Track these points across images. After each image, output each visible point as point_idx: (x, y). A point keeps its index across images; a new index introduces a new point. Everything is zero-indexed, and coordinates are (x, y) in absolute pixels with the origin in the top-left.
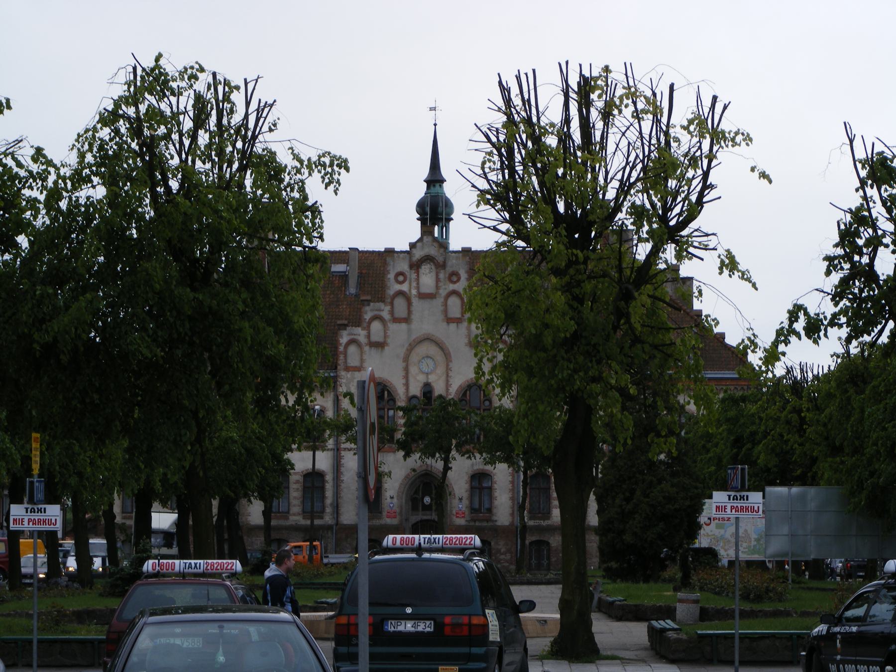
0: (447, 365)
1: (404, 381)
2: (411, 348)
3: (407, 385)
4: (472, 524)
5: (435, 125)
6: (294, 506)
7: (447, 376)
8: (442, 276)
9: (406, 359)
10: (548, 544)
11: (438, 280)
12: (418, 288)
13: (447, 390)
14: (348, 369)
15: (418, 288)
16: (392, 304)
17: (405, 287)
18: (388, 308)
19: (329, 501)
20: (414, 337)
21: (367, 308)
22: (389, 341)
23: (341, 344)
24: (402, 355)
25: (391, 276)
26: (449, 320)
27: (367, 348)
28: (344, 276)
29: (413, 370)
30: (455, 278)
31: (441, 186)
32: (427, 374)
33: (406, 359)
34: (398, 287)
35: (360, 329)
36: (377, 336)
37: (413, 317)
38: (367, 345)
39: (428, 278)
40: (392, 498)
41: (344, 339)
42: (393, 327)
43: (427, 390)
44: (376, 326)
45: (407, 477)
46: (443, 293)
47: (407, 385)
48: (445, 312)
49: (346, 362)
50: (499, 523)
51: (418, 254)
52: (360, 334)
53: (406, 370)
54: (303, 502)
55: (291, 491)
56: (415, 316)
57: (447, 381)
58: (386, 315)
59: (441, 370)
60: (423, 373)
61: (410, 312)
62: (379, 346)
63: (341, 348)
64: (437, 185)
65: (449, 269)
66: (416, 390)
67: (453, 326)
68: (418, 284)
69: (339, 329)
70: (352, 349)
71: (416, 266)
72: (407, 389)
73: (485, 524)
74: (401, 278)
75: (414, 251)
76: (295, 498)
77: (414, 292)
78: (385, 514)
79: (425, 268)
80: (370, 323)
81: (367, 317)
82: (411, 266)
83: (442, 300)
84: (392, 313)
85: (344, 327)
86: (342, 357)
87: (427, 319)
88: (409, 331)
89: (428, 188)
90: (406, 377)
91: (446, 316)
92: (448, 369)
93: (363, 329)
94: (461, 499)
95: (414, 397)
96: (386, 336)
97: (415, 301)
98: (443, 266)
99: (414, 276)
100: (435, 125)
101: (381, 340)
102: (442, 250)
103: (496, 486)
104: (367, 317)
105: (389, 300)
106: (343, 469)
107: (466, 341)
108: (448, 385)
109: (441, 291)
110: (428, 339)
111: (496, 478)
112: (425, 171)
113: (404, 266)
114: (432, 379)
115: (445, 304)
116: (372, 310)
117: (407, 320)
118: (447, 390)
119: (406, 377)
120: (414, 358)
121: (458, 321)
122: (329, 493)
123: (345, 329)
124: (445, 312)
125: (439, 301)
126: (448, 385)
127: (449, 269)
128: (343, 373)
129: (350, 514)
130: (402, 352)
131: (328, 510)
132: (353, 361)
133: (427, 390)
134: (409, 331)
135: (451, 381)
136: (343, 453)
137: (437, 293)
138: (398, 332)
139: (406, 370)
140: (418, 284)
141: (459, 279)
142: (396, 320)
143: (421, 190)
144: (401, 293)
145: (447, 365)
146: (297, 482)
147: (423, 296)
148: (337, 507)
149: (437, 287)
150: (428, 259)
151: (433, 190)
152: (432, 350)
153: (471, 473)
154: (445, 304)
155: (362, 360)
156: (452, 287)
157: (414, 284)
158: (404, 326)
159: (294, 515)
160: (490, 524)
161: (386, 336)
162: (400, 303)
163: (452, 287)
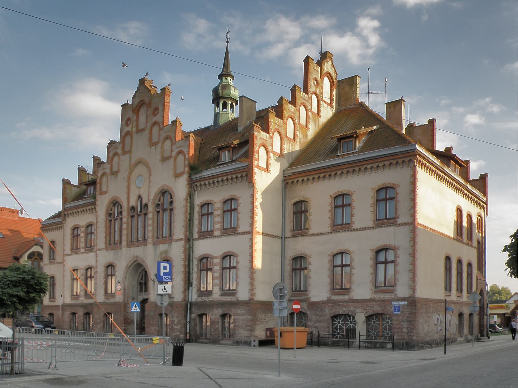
0: (149, 179)
1: (126, 196)
9: (129, 180)
29: (133, 187)
33: (129, 180)
48: (150, 139)
53: (129, 187)
77: (134, 130)
88: (130, 158)
92: (150, 182)
117: (130, 152)
124: (150, 139)
125: (147, 131)
134: (130, 158)
139: (129, 187)
156: (154, 119)
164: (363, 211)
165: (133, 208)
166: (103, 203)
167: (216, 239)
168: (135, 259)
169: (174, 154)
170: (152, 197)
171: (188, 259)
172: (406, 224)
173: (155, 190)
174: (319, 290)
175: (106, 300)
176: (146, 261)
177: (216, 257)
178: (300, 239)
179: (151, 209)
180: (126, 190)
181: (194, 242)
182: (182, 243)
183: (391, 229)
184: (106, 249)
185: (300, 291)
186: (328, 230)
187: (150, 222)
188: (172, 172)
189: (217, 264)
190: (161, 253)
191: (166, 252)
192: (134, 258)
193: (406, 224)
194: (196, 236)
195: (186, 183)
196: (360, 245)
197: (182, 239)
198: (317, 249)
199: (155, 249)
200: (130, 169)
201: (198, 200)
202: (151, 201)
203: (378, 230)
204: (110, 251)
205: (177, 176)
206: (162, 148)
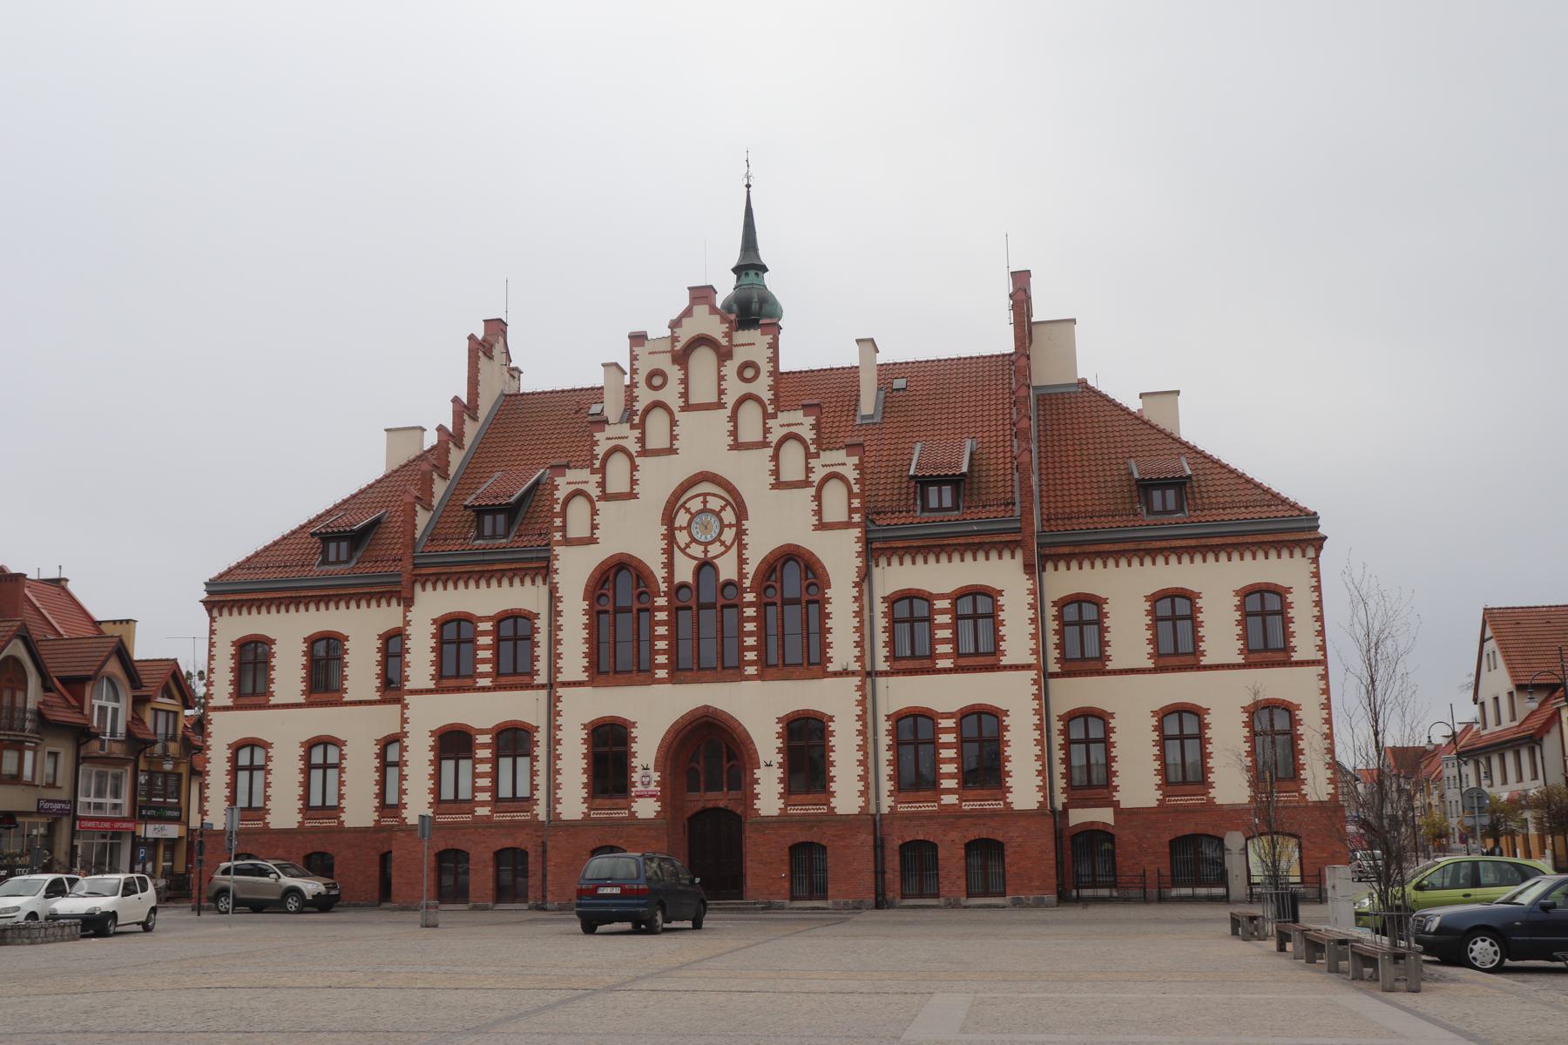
1: (663, 558)
3: (669, 565)
5: (748, 186)
9: (669, 517)
13: (740, 569)
14: (567, 542)
46: (730, 400)
47: (669, 565)
51: (686, 333)
64: (752, 273)
75: (678, 331)
81: (600, 450)
95: (683, 585)
100: (748, 186)
104: (600, 450)
108: (742, 561)
112: (734, 257)
113: (664, 362)
115: (734, 418)
119: (669, 552)
126: (742, 561)
128: (558, 550)
135: (746, 554)
151: (745, 280)
154: (734, 418)
164: (1221, 633)
166: (574, 569)
170: (750, 569)
174: (1138, 782)
185: (1090, 785)
196: (1225, 696)
198: (1133, 703)
202: (750, 576)
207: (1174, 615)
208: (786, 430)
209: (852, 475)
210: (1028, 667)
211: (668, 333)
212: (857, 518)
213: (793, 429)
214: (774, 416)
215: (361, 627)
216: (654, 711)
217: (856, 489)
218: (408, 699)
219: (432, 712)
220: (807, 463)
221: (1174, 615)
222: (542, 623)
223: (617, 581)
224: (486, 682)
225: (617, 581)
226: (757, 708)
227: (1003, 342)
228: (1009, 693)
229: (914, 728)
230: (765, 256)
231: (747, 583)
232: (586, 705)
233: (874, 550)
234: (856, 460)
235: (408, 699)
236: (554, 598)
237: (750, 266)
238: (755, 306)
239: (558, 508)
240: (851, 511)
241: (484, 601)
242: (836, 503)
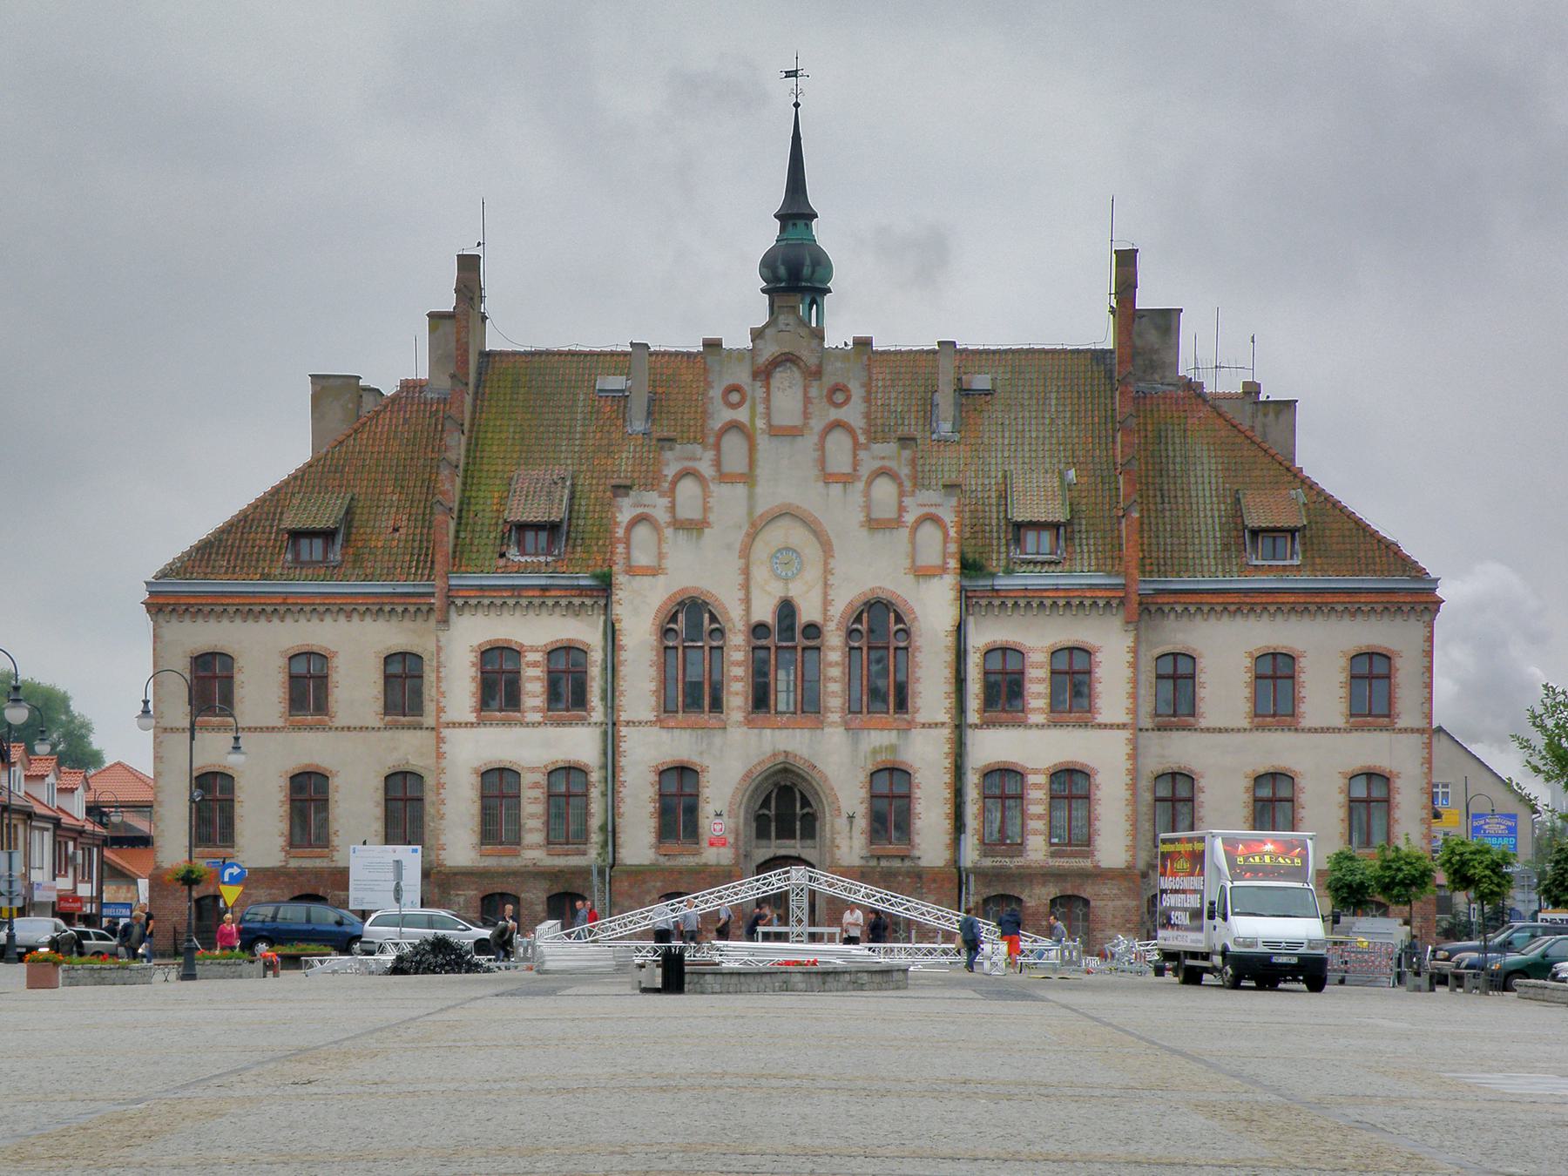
1: (741, 594)
2: (756, 528)
3: (747, 601)
4: (873, 863)
6: (531, 830)
7: (826, 584)
8: (814, 392)
9: (746, 552)
10: (1019, 900)
11: (807, 400)
12: (768, 415)
13: (825, 610)
14: (632, 571)
15: (768, 415)
16: (717, 447)
17: (742, 415)
18: (710, 454)
19: (595, 823)
20: (759, 511)
21: (668, 455)
22: (712, 518)
23: (617, 524)
24: (738, 546)
25: (716, 393)
26: (828, 478)
27: (669, 532)
28: (621, 398)
29: (760, 573)
30: (839, 397)
31: (808, 227)
32: (786, 580)
33: (746, 552)
34: (727, 415)
35: (654, 494)
36: (688, 506)
37: (758, 471)
38: (669, 525)
39: (787, 396)
40: (719, 815)
41: (624, 515)
42: (720, 491)
43: (787, 609)
44: (687, 488)
45: (748, 775)
48: (822, 461)
49: (628, 558)
50: (923, 863)
51: (769, 350)
52: (657, 505)
53: (746, 572)
54: (547, 823)
55: (524, 801)
56: (763, 471)
57: (826, 594)
58: (706, 467)
59: (813, 573)
60: (778, 577)
61: (752, 463)
62: (694, 527)
63: (620, 532)
64: (801, 224)
65: (829, 380)
66: (764, 612)
67: (836, 489)
68: (768, 408)
69: (615, 496)
70: (642, 533)
71: (764, 373)
72: (748, 610)
73: (897, 864)
74: (735, 397)
76: (532, 816)
77: (760, 423)
78: (705, 844)
79: (781, 377)
80: (674, 483)
81: (670, 471)
82: (755, 375)
83: (815, 439)
84: (718, 463)
85: (622, 489)
86: (620, 549)
87: (786, 477)
88: (751, 497)
89: (783, 229)
90: (746, 586)
91: (823, 469)
92: (827, 571)
93: (662, 494)
94: (851, 818)
96: (706, 509)
97: (763, 442)
98: (816, 374)
99: (760, 393)
101: (696, 514)
102: (815, 342)
103: (917, 793)
104: (670, 471)
105: (711, 440)
106: (623, 762)
107: (862, 517)
108: (826, 603)
109: (813, 422)
110: (786, 513)
111: (918, 778)
113: (742, 376)
114: (795, 591)
115: (821, 447)
116: (678, 459)
118: (825, 610)
119: (746, 586)
120: (761, 550)
121: (846, 480)
122: (596, 807)
123: (627, 495)
124: (822, 461)
125: (811, 440)
126: (826, 603)
127: (829, 380)
129: (639, 843)
130: (738, 538)
131: (595, 838)
132: (642, 558)
133: (787, 609)
134: (751, 497)
135: (832, 594)
136: (624, 731)
137: (805, 425)
138: (730, 503)
139: (746, 572)
140: (768, 408)
141: (848, 399)
142: (724, 477)
143: (767, 235)
144: (734, 426)
145: (826, 564)
146: (536, 785)
147: (776, 432)
148: (611, 833)
149: (806, 415)
150: (787, 359)
151: (793, 234)
152: (794, 535)
153: (871, 768)
154: (821, 447)
155: (661, 556)
156: (834, 414)
157: (761, 408)
158: (740, 490)
159: (531, 847)
160: (907, 863)
161: (706, 509)
162: (733, 443)
163: (834, 414)
165: (759, 629)
167: (1035, 733)
168: (781, 758)
169: (910, 518)
171: (958, 770)
172: (1412, 731)
173: (845, 596)
175: (662, 860)
176: (820, 766)
177: (1036, 771)
178: (1176, 735)
179: (834, 639)
180: (740, 579)
181: (969, 732)
182: (946, 732)
183: (1384, 737)
184: (659, 722)
186: (1246, 723)
187: (835, 672)
188: (907, 563)
189: (1037, 786)
190: (875, 752)
191: (893, 748)
192: (774, 755)
193: (1412, 731)
194: (973, 717)
195: (952, 595)
197: (943, 724)
199: (856, 742)
200: (753, 525)
201: (981, 636)
203: (1355, 735)
204: (677, 732)
205: (922, 573)
206: (867, 493)
207: (1276, 677)
208: (877, 464)
209: (949, 518)
210: (1124, 726)
211: (748, 344)
212: (953, 564)
213: (933, 510)
214: (867, 448)
215: (357, 649)
216: (731, 757)
217: (952, 532)
218: (445, 732)
219: (468, 747)
220: (900, 502)
221: (1276, 677)
222: (596, 656)
223: (690, 620)
224: (538, 717)
225: (690, 620)
226: (837, 758)
227: (1100, 334)
228: (1103, 752)
229: (1004, 782)
230: (814, 199)
231: (832, 626)
232: (649, 748)
233: (967, 600)
234: (954, 501)
235: (445, 732)
236: (612, 633)
237: (796, 213)
238: (806, 271)
239: (620, 532)
240: (945, 555)
241: (536, 632)
242: (932, 547)
